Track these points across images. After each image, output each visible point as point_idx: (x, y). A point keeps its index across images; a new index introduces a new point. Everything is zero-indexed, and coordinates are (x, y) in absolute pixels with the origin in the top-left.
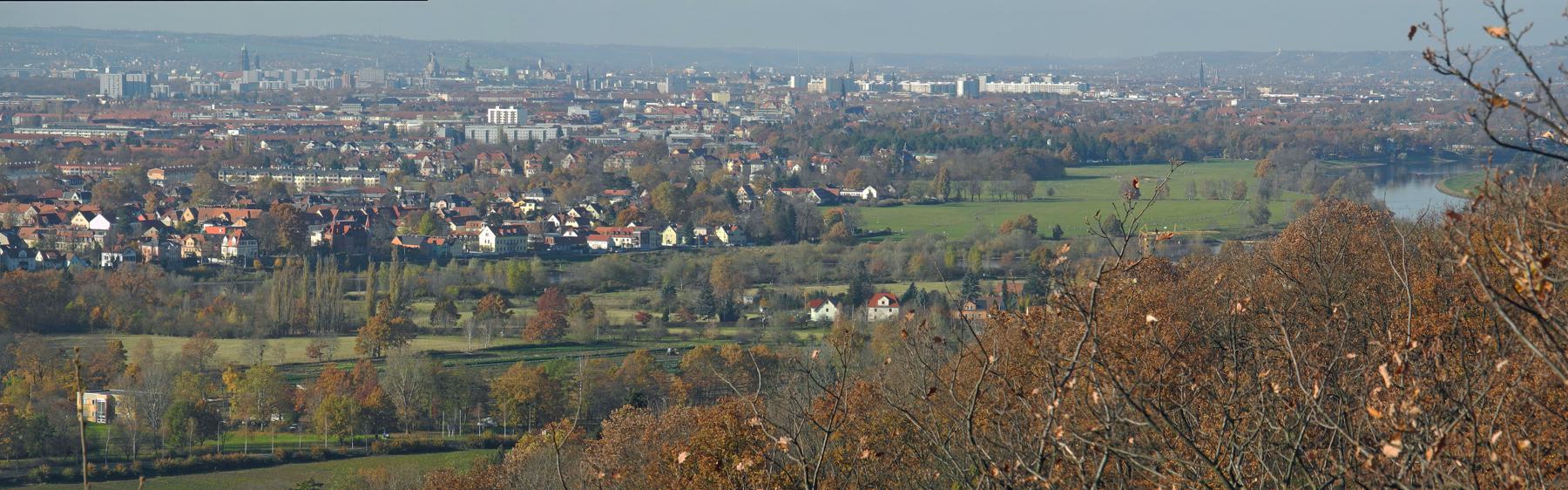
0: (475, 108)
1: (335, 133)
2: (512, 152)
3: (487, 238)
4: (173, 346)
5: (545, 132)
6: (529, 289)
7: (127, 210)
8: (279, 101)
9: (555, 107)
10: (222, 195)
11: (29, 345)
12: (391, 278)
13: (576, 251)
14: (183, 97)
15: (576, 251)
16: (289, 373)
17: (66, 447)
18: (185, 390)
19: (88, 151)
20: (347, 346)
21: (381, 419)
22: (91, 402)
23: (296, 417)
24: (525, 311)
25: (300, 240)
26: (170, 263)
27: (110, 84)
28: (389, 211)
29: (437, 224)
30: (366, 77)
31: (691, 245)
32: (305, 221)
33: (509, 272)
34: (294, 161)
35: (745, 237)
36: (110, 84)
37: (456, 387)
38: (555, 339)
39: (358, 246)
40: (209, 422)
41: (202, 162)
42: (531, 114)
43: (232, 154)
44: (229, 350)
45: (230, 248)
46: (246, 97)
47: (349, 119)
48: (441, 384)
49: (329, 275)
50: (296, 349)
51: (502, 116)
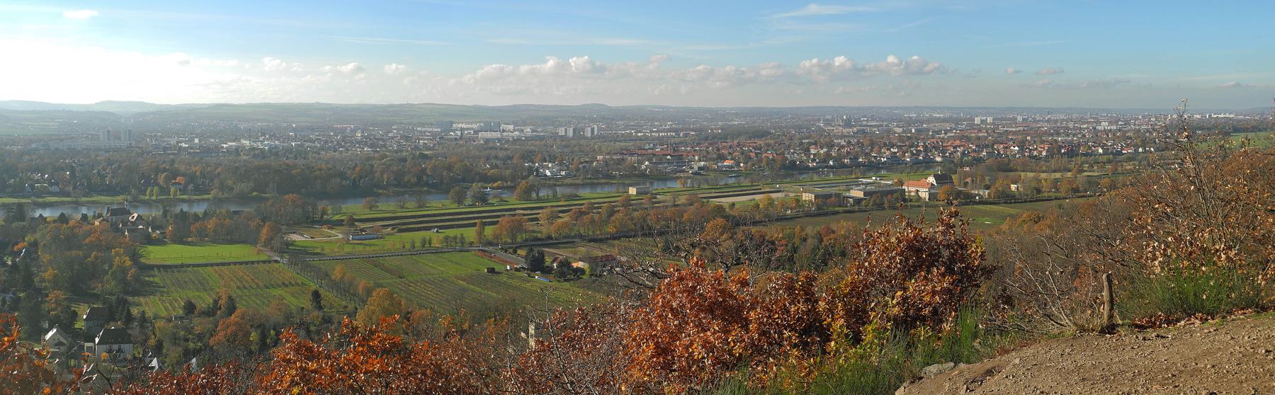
0: (1099, 122)
1: (1068, 128)
2: (1106, 132)
3: (1101, 151)
4: (1031, 175)
5: (1114, 127)
6: (1109, 162)
7: (1022, 145)
8: (1056, 121)
9: (1116, 122)
10: (1043, 142)
11: (1001, 174)
12: (1079, 160)
13: (1120, 153)
14: (1035, 121)
15: (1120, 153)
16: (1057, 180)
17: (1008, 196)
18: (1033, 185)
19: (1014, 133)
20: (1069, 174)
21: (1076, 190)
22: (1013, 187)
23: (1058, 190)
24: (1109, 166)
25: (1059, 151)
26: (1031, 157)
27: (1020, 119)
28: (1079, 145)
29: (1090, 148)
30: (1074, 116)
31: (1145, 152)
32: (1061, 147)
33: (1105, 158)
34: (1058, 134)
35: (1157, 150)
36: (1020, 119)
37: (1092, 183)
38: (1115, 173)
39: (1072, 153)
40: (1039, 191)
41: (1039, 135)
42: (1111, 123)
43: (1045, 133)
44: (1043, 175)
45: (1044, 153)
46: (1049, 121)
47: (1071, 125)
48: (1089, 182)
49: (1065, 159)
50: (1058, 175)
51: (1104, 125)
